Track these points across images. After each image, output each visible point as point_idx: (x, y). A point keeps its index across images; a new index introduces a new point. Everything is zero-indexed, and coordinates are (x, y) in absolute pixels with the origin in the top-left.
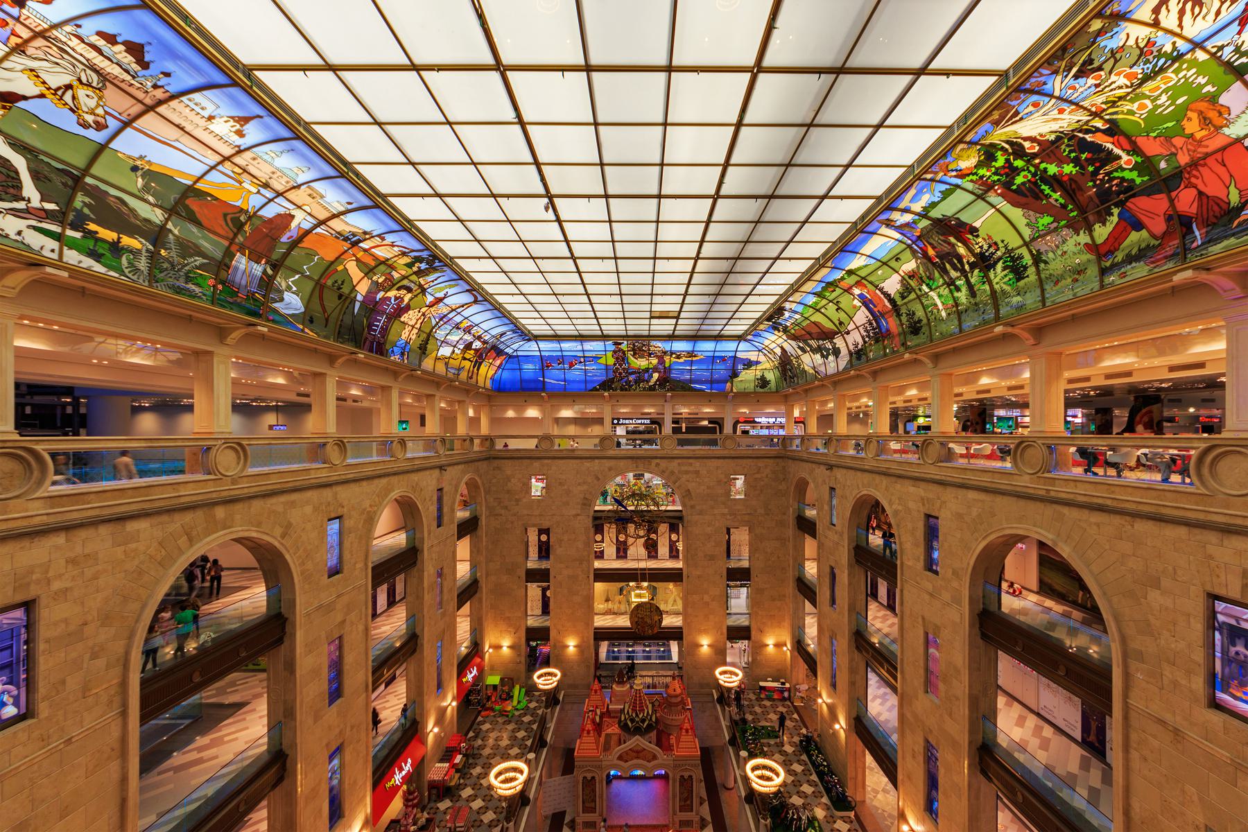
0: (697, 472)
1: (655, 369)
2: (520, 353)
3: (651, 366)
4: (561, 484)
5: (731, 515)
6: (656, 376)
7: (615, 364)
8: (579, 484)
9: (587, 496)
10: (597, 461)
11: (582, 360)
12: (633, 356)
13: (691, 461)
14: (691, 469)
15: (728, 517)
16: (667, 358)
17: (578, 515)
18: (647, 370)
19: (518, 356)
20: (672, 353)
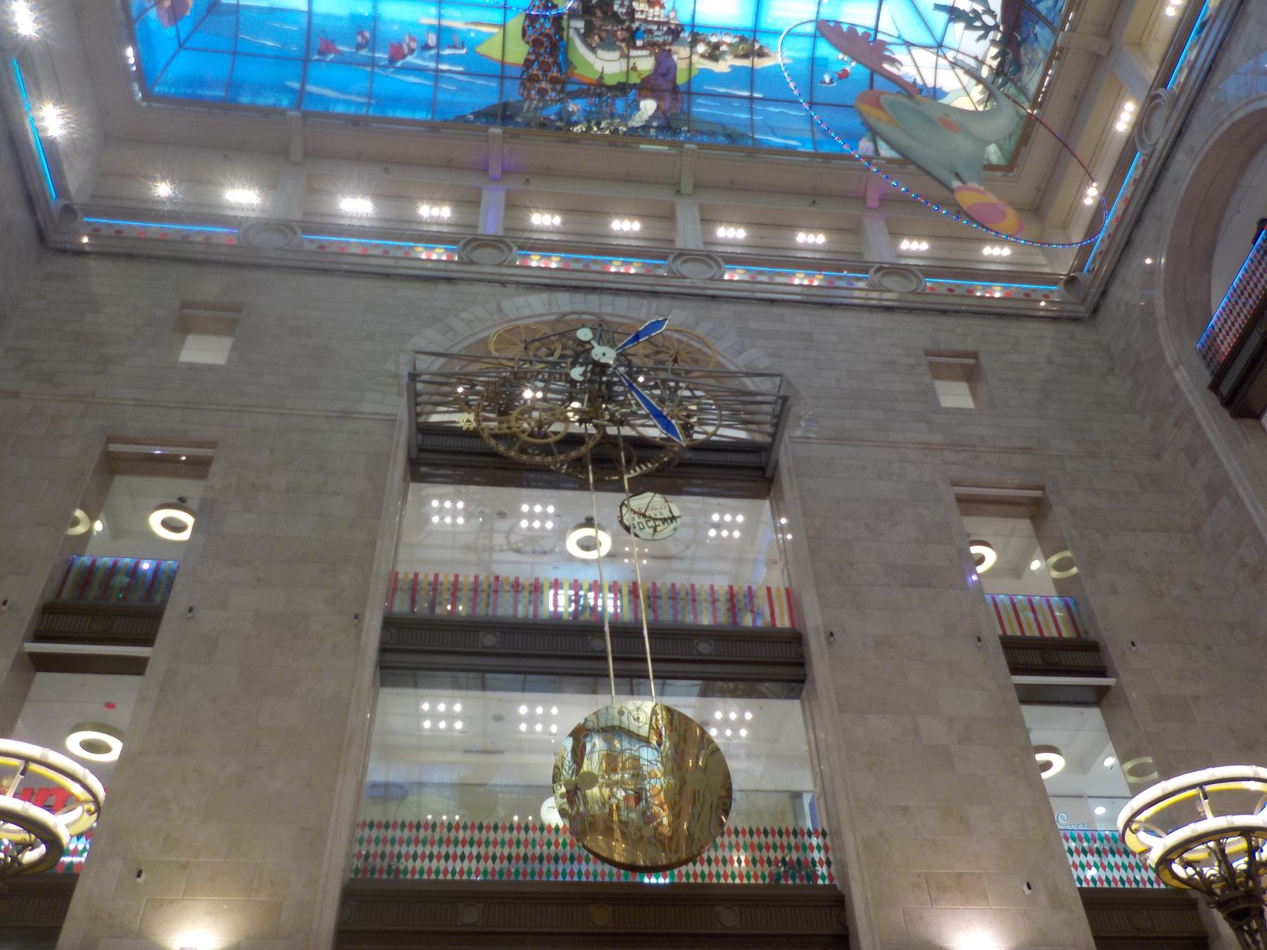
1: (648, 87)
3: (635, 79)
6: (648, 106)
7: (528, 64)
11: (432, 40)
12: (586, 36)
15: (948, 455)
16: (680, 54)
18: (622, 88)
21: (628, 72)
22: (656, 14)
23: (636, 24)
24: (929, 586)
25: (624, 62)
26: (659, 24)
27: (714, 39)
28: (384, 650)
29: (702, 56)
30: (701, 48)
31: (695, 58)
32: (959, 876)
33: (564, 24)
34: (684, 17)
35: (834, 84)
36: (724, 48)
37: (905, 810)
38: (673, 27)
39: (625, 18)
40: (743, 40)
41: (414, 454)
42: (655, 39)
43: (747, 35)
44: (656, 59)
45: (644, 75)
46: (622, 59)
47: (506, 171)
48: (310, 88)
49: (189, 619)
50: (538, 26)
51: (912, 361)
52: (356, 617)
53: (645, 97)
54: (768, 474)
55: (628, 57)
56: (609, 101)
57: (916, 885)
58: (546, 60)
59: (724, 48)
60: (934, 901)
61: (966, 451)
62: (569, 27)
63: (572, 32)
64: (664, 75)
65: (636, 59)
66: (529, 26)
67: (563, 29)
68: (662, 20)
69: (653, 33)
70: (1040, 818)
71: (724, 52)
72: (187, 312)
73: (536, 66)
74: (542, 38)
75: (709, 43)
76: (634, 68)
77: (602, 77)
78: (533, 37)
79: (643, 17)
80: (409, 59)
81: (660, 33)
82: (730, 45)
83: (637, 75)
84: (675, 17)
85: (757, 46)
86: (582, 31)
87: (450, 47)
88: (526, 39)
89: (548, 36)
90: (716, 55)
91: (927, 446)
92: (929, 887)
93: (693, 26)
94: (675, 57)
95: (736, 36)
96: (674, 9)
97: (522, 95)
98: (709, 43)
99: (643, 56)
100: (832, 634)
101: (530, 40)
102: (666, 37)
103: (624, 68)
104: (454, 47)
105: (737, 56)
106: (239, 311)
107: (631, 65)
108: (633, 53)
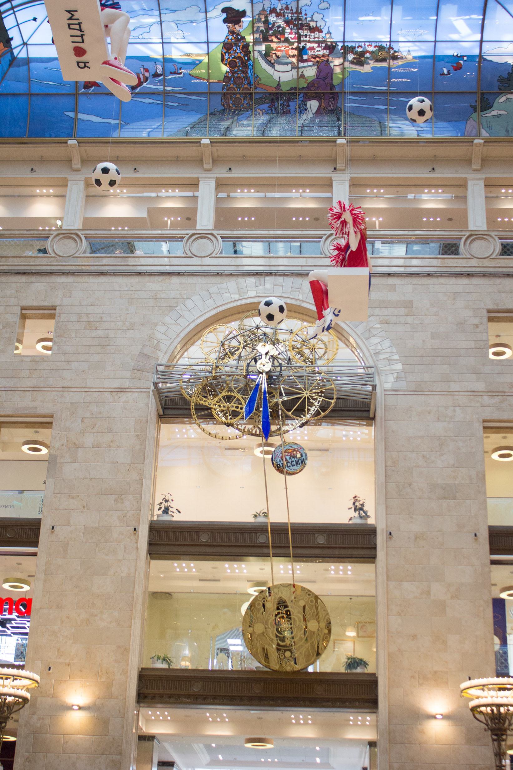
0: (408, 305)
2: (34, 53)
4: (90, 326)
5: (492, 393)
8: (132, 327)
9: (147, 350)
10: (175, 280)
13: (391, 281)
14: (392, 296)
17: (122, 390)
19: (28, 61)
20: (346, 50)
21: (298, 79)
22: (316, 36)
23: (303, 44)
24: (454, 498)
25: (295, 71)
26: (318, 43)
27: (360, 50)
28: (150, 544)
29: (352, 62)
30: (350, 57)
31: (347, 64)
32: (436, 672)
33: (251, 49)
34: (337, 37)
35: (451, 75)
36: (368, 55)
37: (414, 637)
38: (329, 44)
39: (293, 41)
40: (381, 48)
41: (161, 413)
42: (317, 53)
43: (384, 44)
44: (318, 67)
45: (308, 82)
46: (293, 70)
47: (215, 161)
48: (80, 116)
49: (53, 532)
50: (232, 52)
51: (476, 321)
52: (135, 529)
53: (311, 99)
54: (371, 415)
55: (297, 68)
56: (285, 103)
57: (413, 677)
58: (239, 75)
59: (368, 55)
60: (420, 685)
61: (498, 396)
62: (254, 50)
63: (256, 53)
64: (324, 79)
65: (303, 69)
66: (225, 53)
67: (250, 52)
68: (321, 39)
69: (315, 49)
70: (486, 642)
71: (368, 58)
72: (24, 312)
73: (232, 82)
74: (235, 60)
75: (356, 53)
76: (302, 76)
77: (279, 85)
78: (229, 60)
79: (307, 39)
80: (145, 84)
81: (320, 49)
82: (372, 53)
83: (305, 80)
84: (331, 37)
85: (392, 52)
86: (264, 52)
87: (171, 73)
88: (224, 63)
89: (239, 58)
90: (362, 61)
91: (474, 393)
92: (419, 678)
93: (344, 42)
94: (332, 65)
95: (376, 46)
96: (329, 32)
97: (224, 106)
98: (356, 53)
99: (308, 67)
100: (390, 534)
101: (227, 62)
102: (325, 51)
103: (295, 77)
104: (175, 73)
105: (377, 61)
106: (55, 309)
107: (300, 73)
108: (301, 65)
